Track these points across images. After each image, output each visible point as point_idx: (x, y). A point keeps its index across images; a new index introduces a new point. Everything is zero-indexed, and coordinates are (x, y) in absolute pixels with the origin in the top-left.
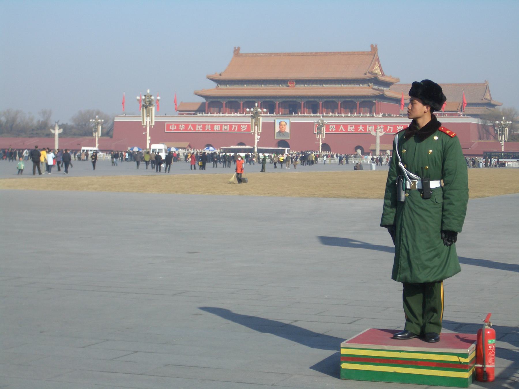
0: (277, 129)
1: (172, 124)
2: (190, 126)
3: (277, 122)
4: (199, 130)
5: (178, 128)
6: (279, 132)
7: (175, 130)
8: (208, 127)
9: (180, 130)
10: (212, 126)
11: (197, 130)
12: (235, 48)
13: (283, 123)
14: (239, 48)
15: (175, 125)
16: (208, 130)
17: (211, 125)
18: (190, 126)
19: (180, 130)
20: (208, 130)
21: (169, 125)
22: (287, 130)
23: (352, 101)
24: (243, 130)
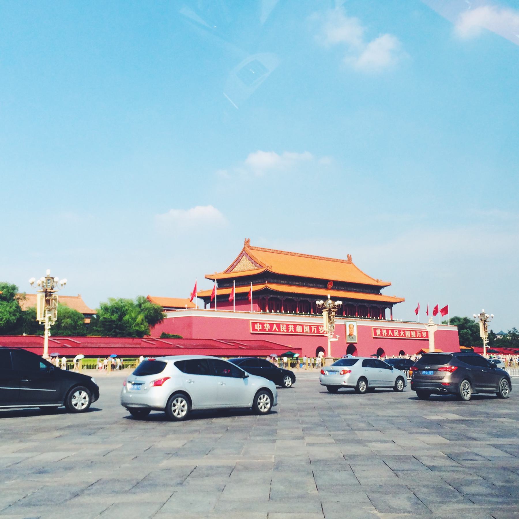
0: (348, 334)
1: (256, 323)
2: (275, 326)
3: (348, 324)
4: (283, 332)
5: (263, 329)
6: (350, 335)
7: (260, 330)
8: (291, 328)
9: (265, 330)
10: (295, 326)
11: (282, 331)
12: (246, 239)
13: (351, 326)
14: (249, 240)
15: (260, 323)
16: (292, 331)
17: (294, 325)
18: (275, 326)
19: (265, 330)
20: (292, 331)
21: (254, 324)
22: (355, 333)
23: (376, 307)
24: (321, 332)
